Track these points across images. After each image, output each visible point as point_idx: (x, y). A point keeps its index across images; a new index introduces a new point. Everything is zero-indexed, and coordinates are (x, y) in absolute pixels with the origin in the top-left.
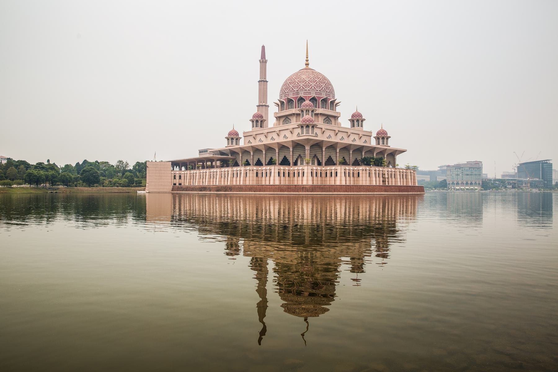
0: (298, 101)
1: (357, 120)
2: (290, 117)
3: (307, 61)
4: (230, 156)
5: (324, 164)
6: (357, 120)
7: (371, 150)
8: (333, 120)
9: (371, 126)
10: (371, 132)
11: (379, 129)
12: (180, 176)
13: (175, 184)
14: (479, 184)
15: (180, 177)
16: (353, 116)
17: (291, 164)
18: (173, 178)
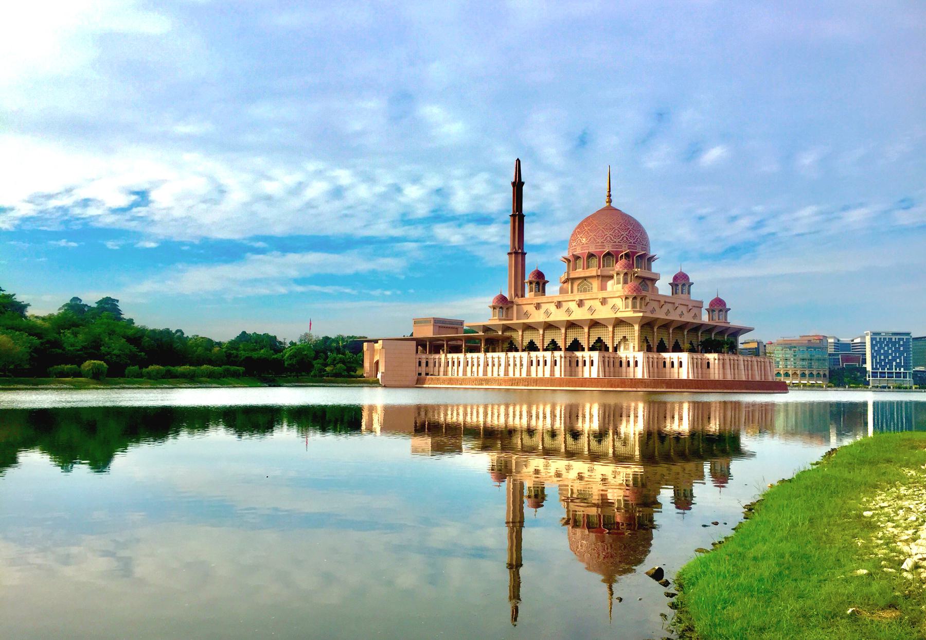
0: (604, 256)
1: (681, 282)
2: (589, 280)
3: (610, 196)
4: (481, 333)
5: (655, 349)
6: (681, 282)
7: (709, 329)
8: (649, 283)
12: (427, 363)
13: (420, 374)
14: (825, 375)
16: (675, 278)
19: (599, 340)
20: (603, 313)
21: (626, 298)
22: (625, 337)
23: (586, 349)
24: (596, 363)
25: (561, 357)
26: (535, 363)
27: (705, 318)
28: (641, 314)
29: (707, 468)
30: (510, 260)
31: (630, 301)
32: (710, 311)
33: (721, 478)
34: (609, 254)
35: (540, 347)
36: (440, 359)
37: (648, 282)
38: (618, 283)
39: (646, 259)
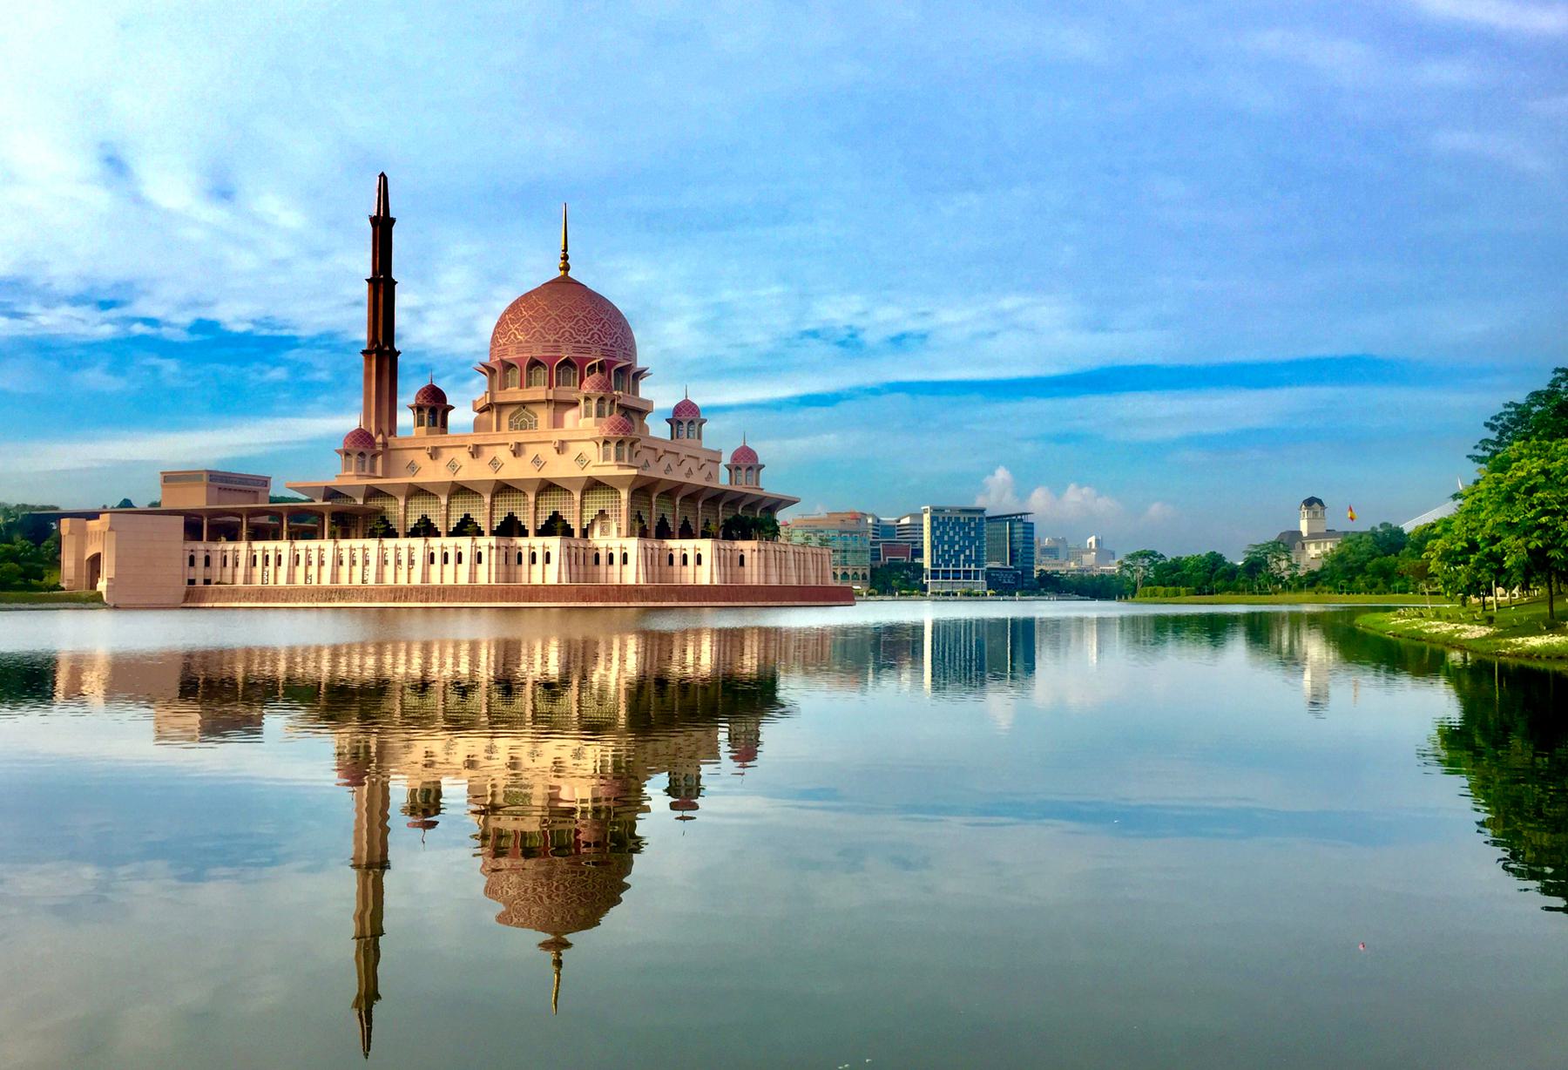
2: (532, 408)
3: (566, 258)
5: (653, 533)
8: (635, 418)
9: (719, 437)
10: (719, 453)
11: (739, 444)
13: (192, 582)
14: (864, 577)
15: (207, 561)
17: (531, 533)
18: (187, 562)
19: (556, 517)
20: (560, 468)
21: (606, 442)
22: (602, 512)
23: (531, 533)
24: (554, 558)
25: (491, 548)
26: (438, 559)
27: (723, 480)
28: (634, 472)
29: (723, 736)
30: (368, 365)
31: (612, 447)
32: (733, 468)
33: (746, 752)
34: (567, 363)
35: (485, 527)
36: (235, 551)
37: (635, 413)
38: (587, 415)
39: (630, 375)
